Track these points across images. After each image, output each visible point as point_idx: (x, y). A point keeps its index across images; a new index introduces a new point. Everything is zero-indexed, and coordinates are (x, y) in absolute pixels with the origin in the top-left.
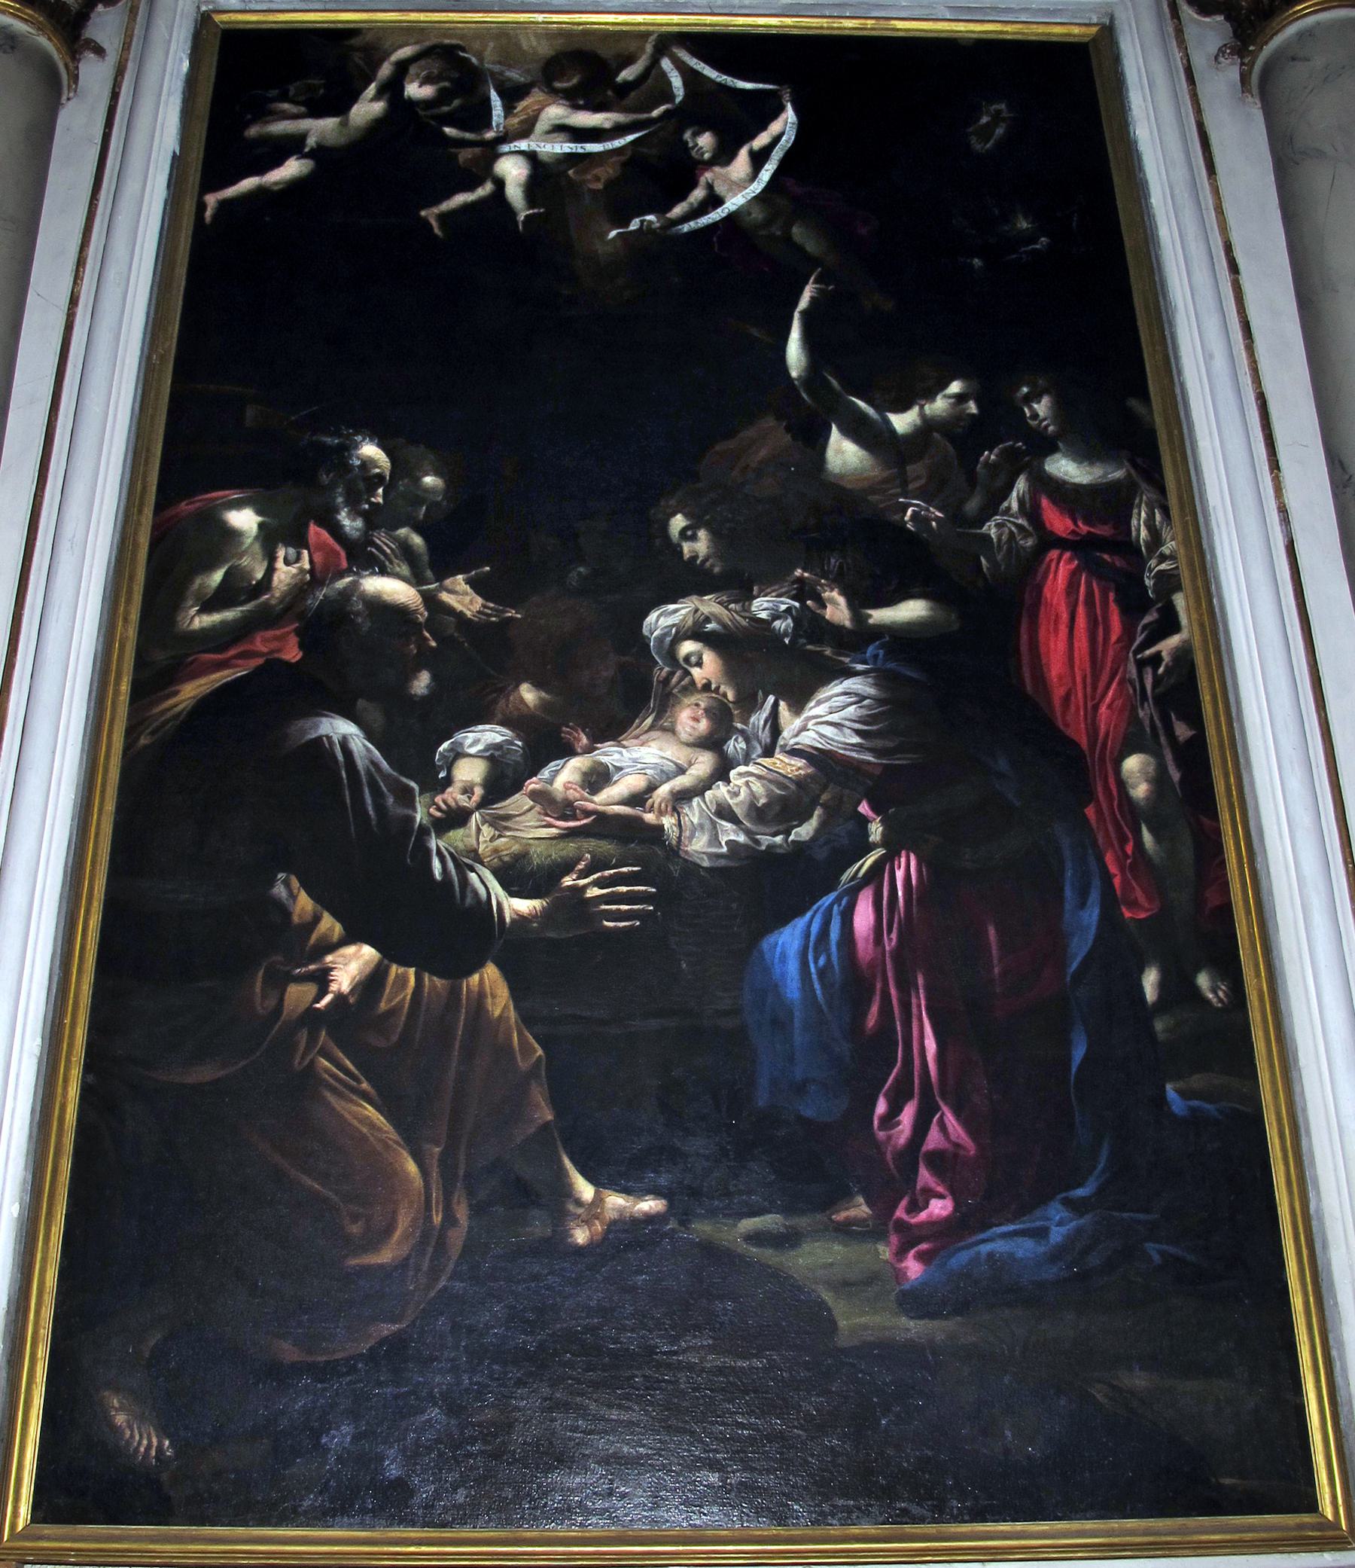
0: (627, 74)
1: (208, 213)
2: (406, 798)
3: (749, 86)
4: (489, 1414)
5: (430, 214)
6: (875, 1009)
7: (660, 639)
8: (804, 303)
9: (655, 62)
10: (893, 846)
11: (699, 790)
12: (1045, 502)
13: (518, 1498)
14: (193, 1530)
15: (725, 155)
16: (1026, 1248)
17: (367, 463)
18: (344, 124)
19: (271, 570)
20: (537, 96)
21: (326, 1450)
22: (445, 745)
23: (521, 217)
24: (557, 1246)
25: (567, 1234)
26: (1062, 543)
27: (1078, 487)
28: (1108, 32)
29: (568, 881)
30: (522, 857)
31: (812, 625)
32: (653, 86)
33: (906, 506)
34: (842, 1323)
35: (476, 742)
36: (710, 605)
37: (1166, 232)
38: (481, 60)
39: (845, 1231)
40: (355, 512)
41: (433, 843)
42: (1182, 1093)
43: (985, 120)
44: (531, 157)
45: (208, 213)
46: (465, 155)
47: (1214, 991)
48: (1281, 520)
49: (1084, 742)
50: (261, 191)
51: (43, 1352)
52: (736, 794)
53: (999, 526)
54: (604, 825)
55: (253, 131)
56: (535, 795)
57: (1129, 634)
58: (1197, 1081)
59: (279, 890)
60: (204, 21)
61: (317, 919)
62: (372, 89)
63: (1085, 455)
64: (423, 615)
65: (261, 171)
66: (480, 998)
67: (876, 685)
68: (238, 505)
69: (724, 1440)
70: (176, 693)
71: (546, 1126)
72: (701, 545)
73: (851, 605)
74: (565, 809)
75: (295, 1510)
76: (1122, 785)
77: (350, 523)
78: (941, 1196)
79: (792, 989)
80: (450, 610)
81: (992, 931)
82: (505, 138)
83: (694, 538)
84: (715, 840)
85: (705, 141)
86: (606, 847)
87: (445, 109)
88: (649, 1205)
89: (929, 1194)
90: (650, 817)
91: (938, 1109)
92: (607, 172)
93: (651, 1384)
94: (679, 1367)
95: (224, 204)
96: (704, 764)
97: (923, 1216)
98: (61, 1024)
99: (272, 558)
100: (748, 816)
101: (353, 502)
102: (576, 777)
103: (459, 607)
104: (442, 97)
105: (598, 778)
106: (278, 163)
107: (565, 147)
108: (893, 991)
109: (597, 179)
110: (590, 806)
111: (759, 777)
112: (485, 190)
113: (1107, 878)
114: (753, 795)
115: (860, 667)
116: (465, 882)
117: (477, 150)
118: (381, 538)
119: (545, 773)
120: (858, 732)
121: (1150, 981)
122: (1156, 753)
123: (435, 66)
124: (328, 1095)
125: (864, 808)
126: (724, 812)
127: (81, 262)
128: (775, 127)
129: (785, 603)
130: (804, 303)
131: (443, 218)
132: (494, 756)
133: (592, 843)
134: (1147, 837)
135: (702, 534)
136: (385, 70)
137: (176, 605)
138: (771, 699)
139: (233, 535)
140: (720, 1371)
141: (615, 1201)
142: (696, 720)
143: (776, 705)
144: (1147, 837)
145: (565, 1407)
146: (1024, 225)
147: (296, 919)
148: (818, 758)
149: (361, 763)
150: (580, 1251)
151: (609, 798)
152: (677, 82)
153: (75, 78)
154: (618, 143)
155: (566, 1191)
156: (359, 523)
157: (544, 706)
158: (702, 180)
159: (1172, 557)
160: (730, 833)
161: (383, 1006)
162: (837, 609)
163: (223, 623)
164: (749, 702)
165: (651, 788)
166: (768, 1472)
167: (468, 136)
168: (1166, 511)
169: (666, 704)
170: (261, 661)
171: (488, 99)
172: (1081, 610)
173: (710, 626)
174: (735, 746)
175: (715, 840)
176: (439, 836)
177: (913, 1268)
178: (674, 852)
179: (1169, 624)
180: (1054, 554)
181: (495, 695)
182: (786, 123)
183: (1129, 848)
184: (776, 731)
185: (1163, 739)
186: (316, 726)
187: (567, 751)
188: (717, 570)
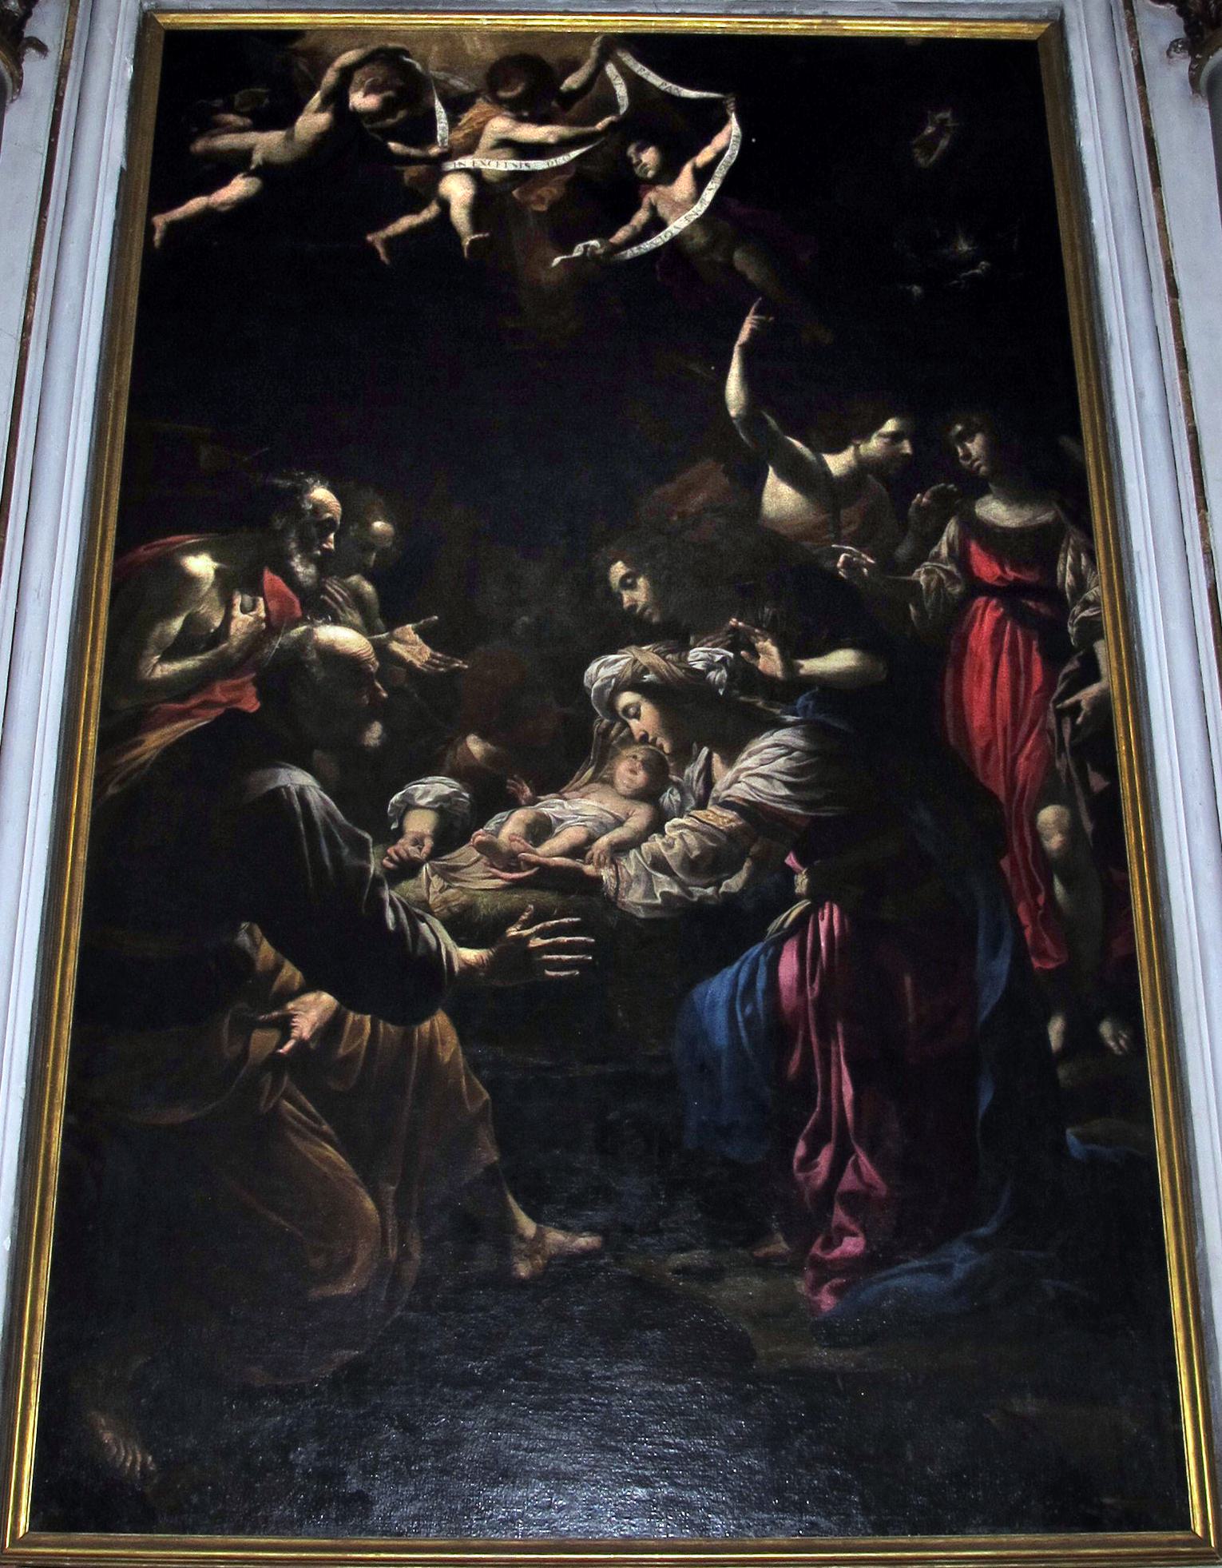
0: (572, 82)
1: (157, 237)
2: (361, 849)
3: (693, 94)
4: (440, 1434)
5: (376, 238)
6: (797, 1056)
7: (601, 690)
8: (744, 335)
9: (599, 69)
10: (818, 897)
11: (635, 842)
12: (974, 547)
13: (468, 1510)
14: (176, 1537)
15: (668, 173)
16: (931, 1283)
17: (319, 507)
18: (290, 138)
19: (228, 619)
20: (481, 107)
21: (292, 1466)
22: (397, 797)
23: (466, 243)
24: (503, 1280)
25: (510, 1268)
26: (990, 591)
27: (1006, 532)
28: (1058, 27)
29: (513, 932)
30: (468, 909)
31: (745, 675)
32: (596, 94)
33: (840, 552)
34: (761, 1352)
35: (426, 793)
36: (647, 655)
37: (1105, 256)
38: (425, 66)
39: (764, 1266)
40: (309, 559)
41: (387, 894)
42: (1083, 1139)
43: (930, 130)
44: (475, 175)
45: (157, 237)
46: (411, 172)
47: (1116, 1038)
48: (1205, 562)
49: (1002, 794)
50: (208, 213)
51: (36, 1376)
52: (670, 846)
53: (927, 572)
54: (546, 877)
55: (200, 145)
56: (482, 847)
57: (1049, 684)
58: (1097, 1126)
59: (243, 939)
60: (146, 21)
61: (278, 968)
62: (317, 98)
63: (1014, 498)
64: (374, 666)
65: (208, 190)
66: (431, 1045)
67: (805, 737)
68: (194, 550)
69: (652, 1459)
70: (141, 743)
71: (490, 1169)
72: (639, 595)
73: (782, 653)
74: (507, 860)
75: (266, 1519)
76: (1036, 836)
77: (303, 570)
78: (854, 1235)
79: (721, 1037)
80: (399, 660)
81: (908, 980)
82: (448, 155)
83: (633, 587)
84: (649, 892)
85: (649, 157)
86: (549, 898)
87: (390, 121)
88: (585, 1241)
89: (843, 1232)
90: (589, 869)
91: (853, 1152)
92: (550, 192)
93: (589, 1407)
94: (611, 1391)
95: (172, 226)
96: (640, 816)
97: (837, 1253)
98: (44, 1069)
99: (228, 606)
100: (682, 868)
101: (306, 547)
102: (520, 829)
103: (408, 657)
104: (387, 108)
105: (541, 830)
106: (225, 181)
107: (506, 164)
108: (814, 1039)
109: (541, 200)
110: (533, 858)
111: (693, 829)
112: (430, 212)
113: (1019, 929)
114: (687, 849)
115: (790, 718)
116: (416, 931)
117: (422, 168)
118: (334, 587)
119: (491, 825)
120: (786, 784)
121: (1055, 1029)
122: (1068, 802)
123: (379, 72)
124: (294, 1139)
125: (791, 860)
126: (659, 864)
127: (32, 287)
128: (719, 141)
129: (721, 653)
130: (744, 335)
131: (389, 242)
132: (443, 808)
133: (534, 895)
134: (1058, 888)
135: (641, 582)
136: (330, 78)
137: (136, 655)
138: (705, 751)
139: (191, 580)
140: (650, 1395)
141: (555, 1237)
142: (634, 772)
143: (709, 757)
144: (1058, 888)
145: (510, 1427)
146: (964, 247)
147: (259, 967)
148: (748, 810)
149: (317, 814)
150: (522, 1284)
151: (551, 850)
152: (621, 90)
153: (18, 83)
154: (562, 160)
155: (508, 1227)
156: (312, 570)
157: (490, 758)
158: (646, 201)
159: (1096, 603)
160: (665, 885)
161: (342, 1052)
162: (770, 659)
163: (183, 672)
164: (684, 755)
165: (591, 839)
166: (693, 1488)
167: (414, 152)
168: (1092, 556)
169: (606, 757)
170: (220, 711)
171: (432, 111)
172: (1005, 658)
173: (647, 677)
174: (671, 798)
175: (649, 892)
176: (391, 887)
177: (827, 1301)
178: (611, 903)
179: (1090, 672)
180: (980, 601)
181: (443, 746)
182: (730, 136)
183: (1041, 899)
184: (709, 783)
185: (1078, 790)
186: (275, 777)
187: (512, 803)
188: (655, 619)
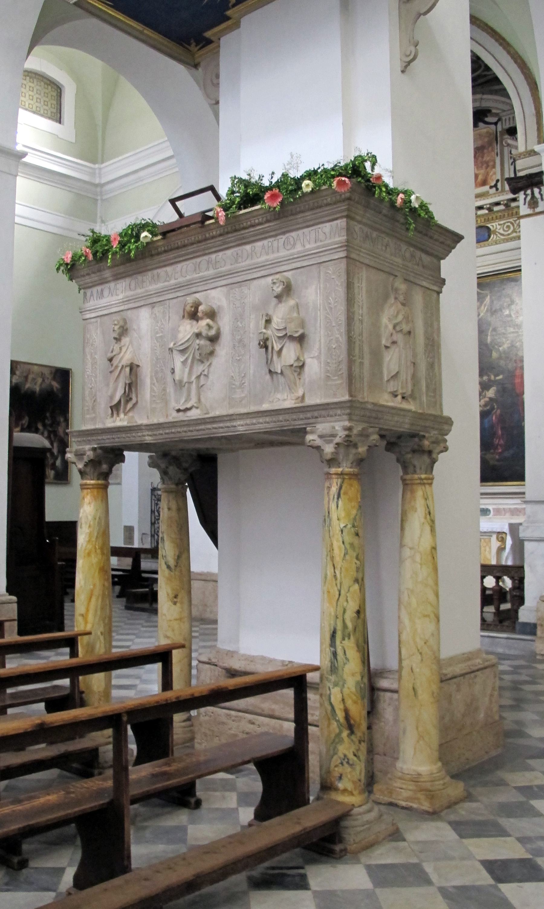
10: (498, 408)
31: (490, 380)
162: (492, 377)
164: (483, 391)
184: (485, 394)
